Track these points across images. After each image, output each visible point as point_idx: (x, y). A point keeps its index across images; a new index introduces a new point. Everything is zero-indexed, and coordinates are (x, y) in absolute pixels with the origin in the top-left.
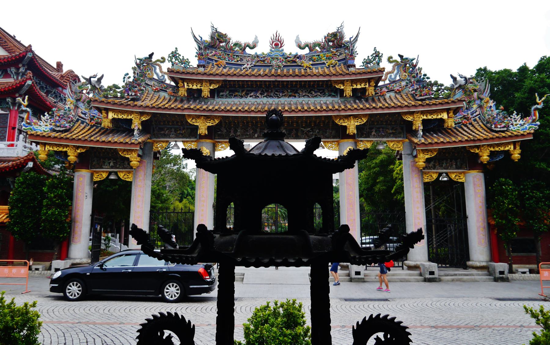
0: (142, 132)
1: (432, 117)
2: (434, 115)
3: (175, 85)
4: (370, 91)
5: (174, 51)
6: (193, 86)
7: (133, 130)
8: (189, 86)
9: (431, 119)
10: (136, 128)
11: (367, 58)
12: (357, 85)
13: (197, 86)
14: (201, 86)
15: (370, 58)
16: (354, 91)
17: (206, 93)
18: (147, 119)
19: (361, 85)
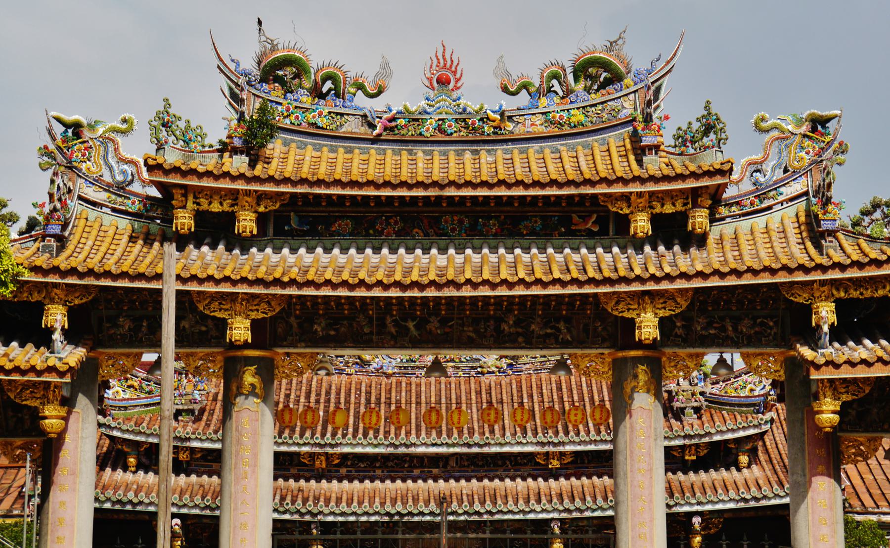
0: (72, 336)
1: (861, 294)
2: (867, 289)
3: (160, 196)
4: (699, 220)
5: (162, 109)
6: (210, 203)
7: (50, 331)
8: (198, 204)
9: (858, 298)
10: (58, 326)
11: (684, 128)
12: (663, 206)
13: (221, 204)
14: (232, 205)
15: (696, 126)
16: (655, 220)
17: (247, 223)
18: (84, 300)
19: (674, 205)
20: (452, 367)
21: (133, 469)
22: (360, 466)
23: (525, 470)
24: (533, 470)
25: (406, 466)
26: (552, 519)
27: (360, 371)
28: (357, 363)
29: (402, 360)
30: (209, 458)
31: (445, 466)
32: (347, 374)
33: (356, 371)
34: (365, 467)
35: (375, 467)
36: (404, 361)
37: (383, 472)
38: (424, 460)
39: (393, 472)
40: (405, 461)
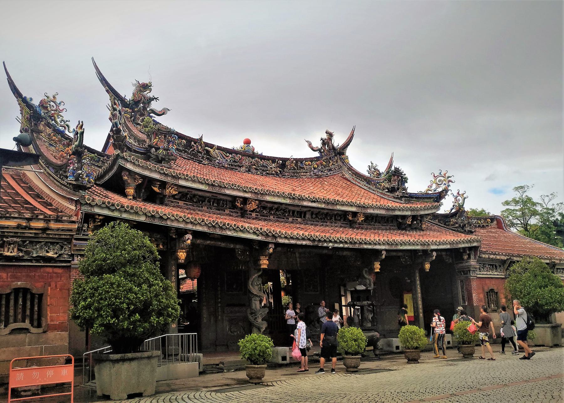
20: (255, 168)
21: (131, 197)
22: (264, 213)
23: (339, 224)
24: (342, 224)
25: (286, 215)
26: (382, 250)
27: (210, 163)
28: (208, 159)
29: (230, 161)
30: (176, 197)
31: (305, 217)
32: (203, 164)
33: (208, 163)
34: (266, 213)
35: (271, 213)
36: (232, 161)
37: (274, 217)
38: (295, 212)
39: (279, 218)
40: (286, 212)
